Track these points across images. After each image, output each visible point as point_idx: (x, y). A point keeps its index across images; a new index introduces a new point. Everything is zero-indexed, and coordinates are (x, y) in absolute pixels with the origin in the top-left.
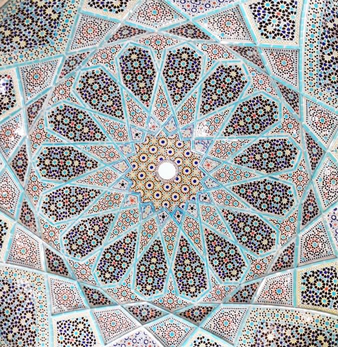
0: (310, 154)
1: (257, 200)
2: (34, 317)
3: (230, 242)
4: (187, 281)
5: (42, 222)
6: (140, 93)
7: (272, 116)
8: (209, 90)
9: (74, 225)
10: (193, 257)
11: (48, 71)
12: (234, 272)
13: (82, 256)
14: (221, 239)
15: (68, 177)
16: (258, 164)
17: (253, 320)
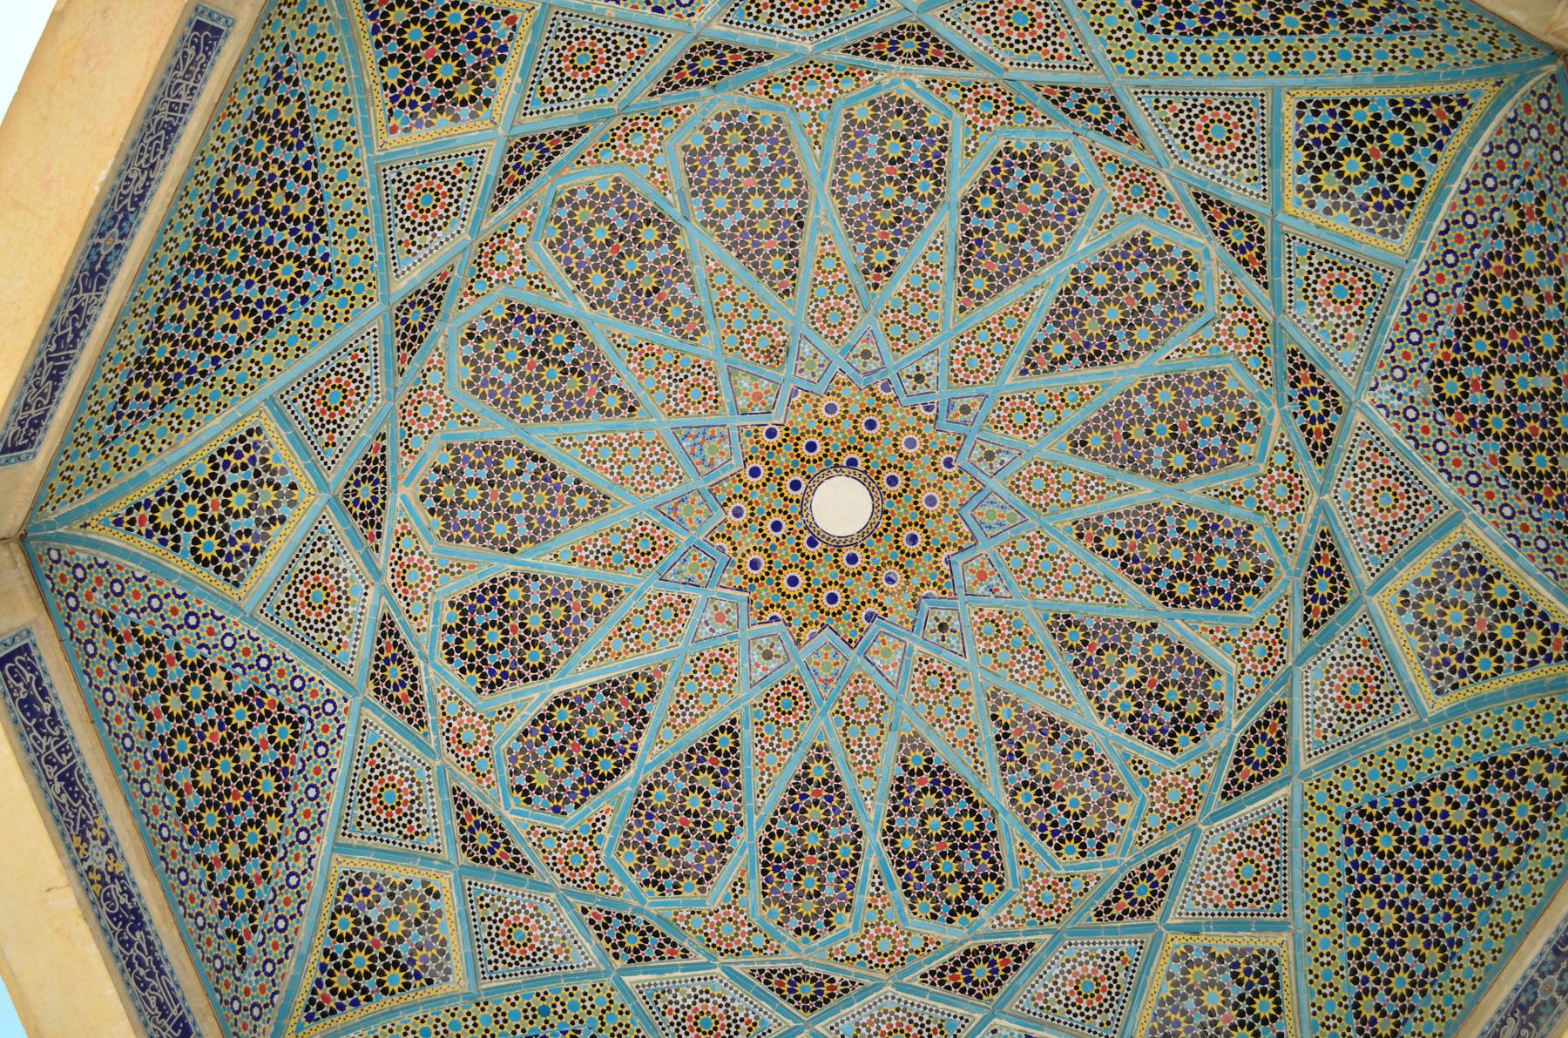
0: (550, 158)
2: (1438, 781)
3: (959, 219)
5: (1146, 837)
8: (530, 526)
9: (1123, 736)
10: (1068, 306)
11: (679, 998)
13: (1212, 673)
15: (981, 811)
16: (667, 270)
17: (1155, 58)
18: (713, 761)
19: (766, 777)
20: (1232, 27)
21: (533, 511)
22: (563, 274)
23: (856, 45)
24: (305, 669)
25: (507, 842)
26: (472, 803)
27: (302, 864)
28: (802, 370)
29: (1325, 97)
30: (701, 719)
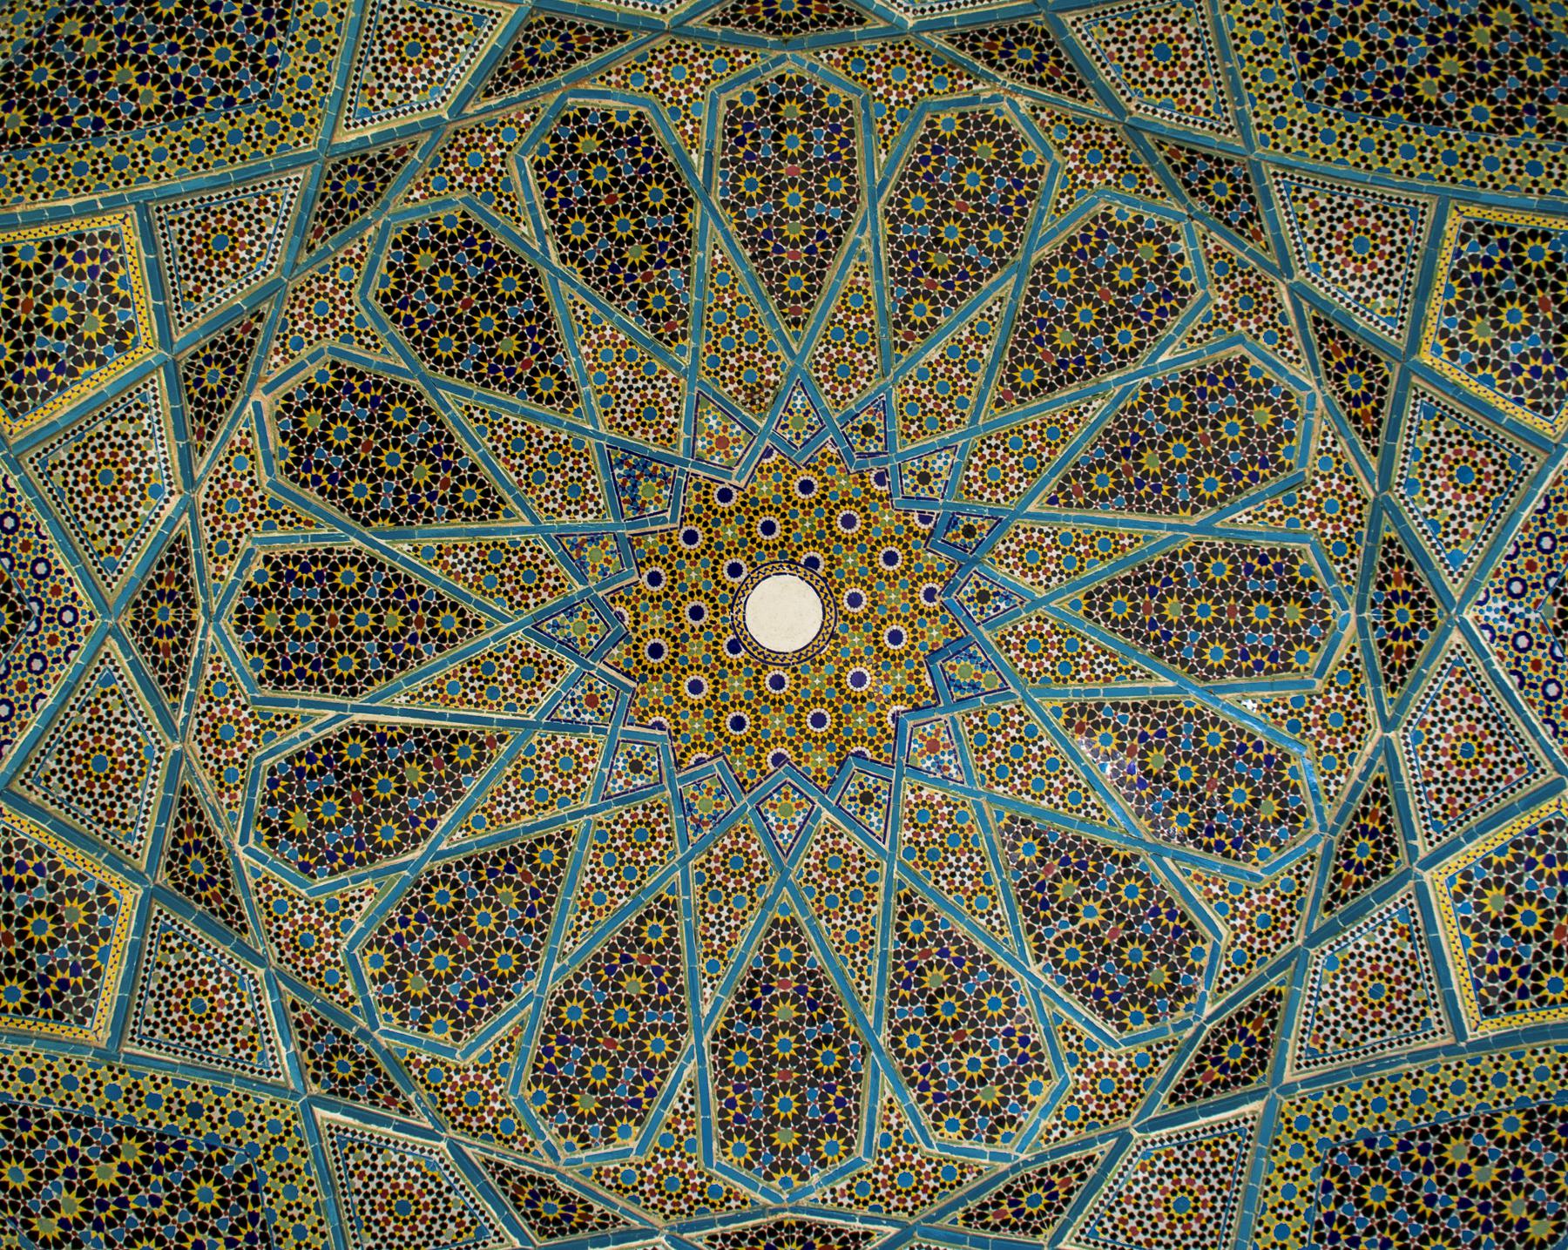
0: (571, 60)
1: (820, 219)
3: (1025, 290)
4: (1234, 446)
5: (1056, 1133)
6: (449, 776)
7: (453, 238)
8: (397, 501)
9: (1059, 991)
11: (379, 1162)
12: (1148, 251)
16: (663, 246)
19: (585, 918)
21: (407, 484)
22: (540, 207)
23: (964, 35)
25: (227, 884)
26: (201, 816)
30: (527, 817)
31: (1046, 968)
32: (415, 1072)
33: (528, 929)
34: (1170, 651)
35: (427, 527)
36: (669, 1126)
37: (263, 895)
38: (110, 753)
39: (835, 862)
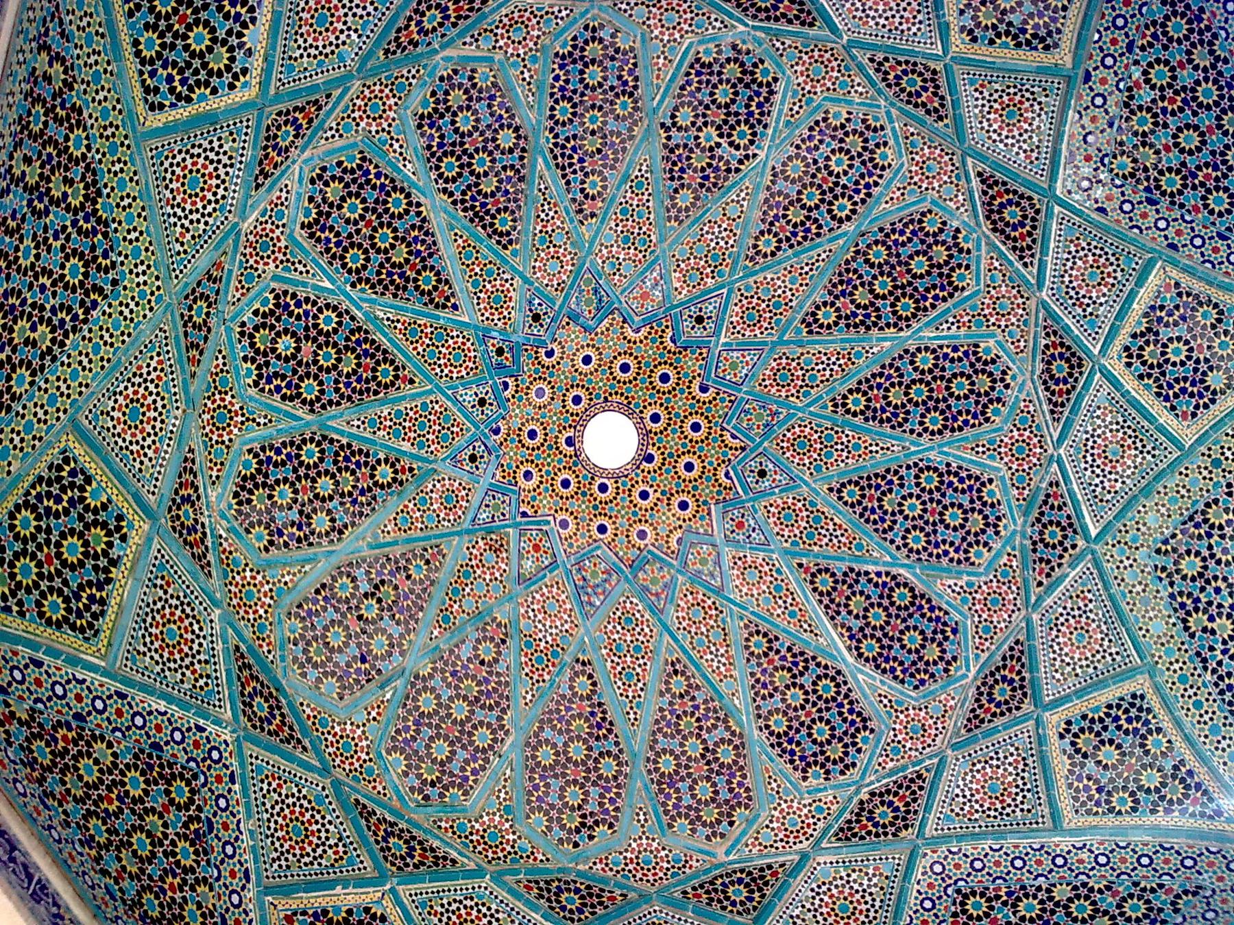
3: (333, 410)
4: (364, 201)
5: (860, 89)
6: (844, 582)
8: (715, 726)
9: (770, 131)
11: (1097, 481)
13: (698, 60)
14: (361, 393)
16: (454, 674)
17: (141, 268)
18: (871, 499)
20: (95, 202)
21: (700, 728)
22: (488, 772)
24: (913, 901)
25: (998, 669)
26: (973, 710)
27: (1084, 855)
28: (503, 515)
29: (138, 85)
31: (758, 147)
32: (1026, 492)
33: (901, 478)
34: (518, 171)
35: (715, 697)
36: (969, 327)
37: (987, 644)
38: (983, 787)
39: (750, 318)
